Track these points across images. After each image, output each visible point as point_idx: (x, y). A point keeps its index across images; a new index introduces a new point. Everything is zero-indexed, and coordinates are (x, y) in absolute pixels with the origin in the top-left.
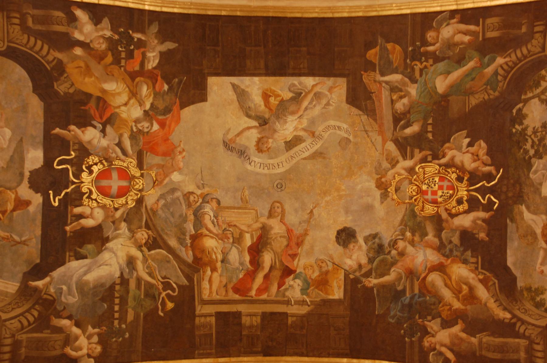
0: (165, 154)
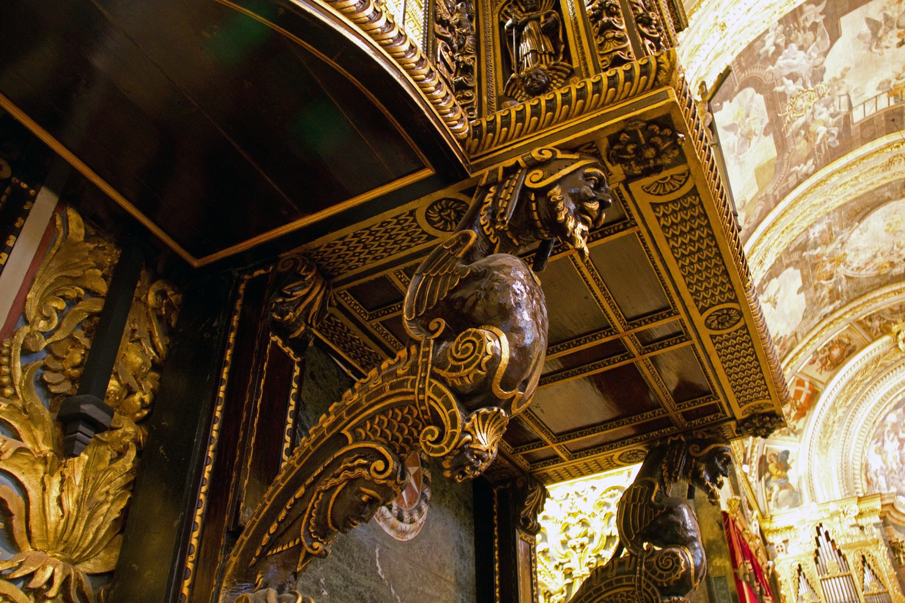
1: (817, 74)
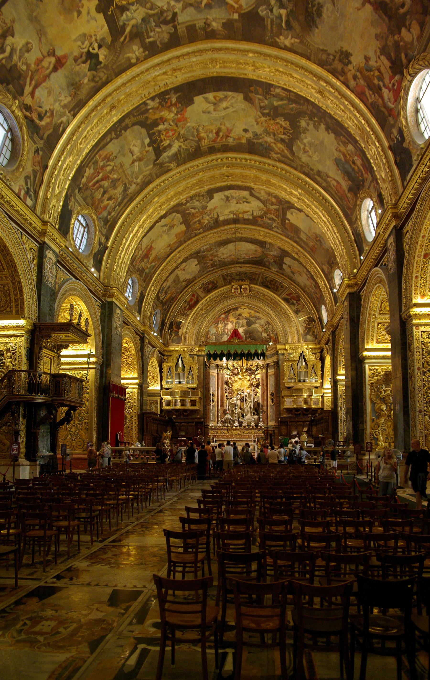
0: (184, 121)
1: (204, 207)
